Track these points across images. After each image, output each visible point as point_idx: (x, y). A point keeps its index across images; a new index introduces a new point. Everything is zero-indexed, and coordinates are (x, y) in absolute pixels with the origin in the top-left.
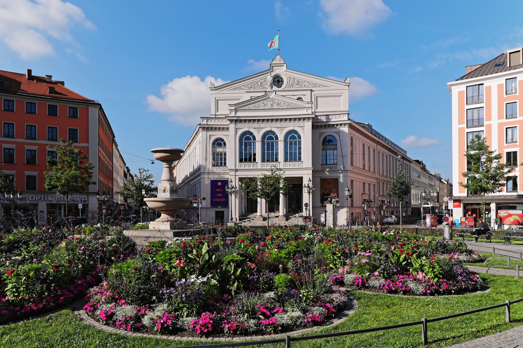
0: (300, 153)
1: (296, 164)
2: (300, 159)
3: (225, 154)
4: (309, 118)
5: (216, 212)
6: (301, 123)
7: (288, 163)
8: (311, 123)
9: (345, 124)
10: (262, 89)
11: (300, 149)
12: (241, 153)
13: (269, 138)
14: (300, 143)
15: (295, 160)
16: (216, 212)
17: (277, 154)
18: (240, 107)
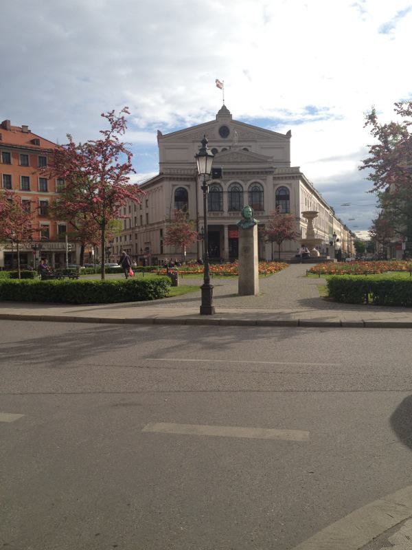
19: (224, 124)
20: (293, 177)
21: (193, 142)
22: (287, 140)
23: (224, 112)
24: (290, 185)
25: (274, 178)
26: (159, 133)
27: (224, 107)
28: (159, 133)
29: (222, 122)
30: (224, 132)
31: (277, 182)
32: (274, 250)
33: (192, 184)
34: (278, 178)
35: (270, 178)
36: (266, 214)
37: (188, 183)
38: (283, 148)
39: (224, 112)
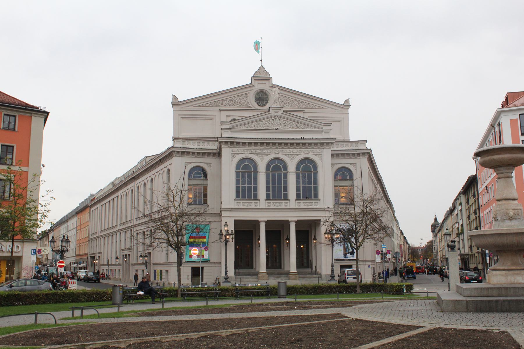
0: (316, 189)
1: (313, 204)
2: (316, 196)
3: (205, 189)
4: (328, 144)
5: (192, 268)
6: (317, 150)
7: (302, 201)
8: (330, 150)
9: (363, 154)
10: (240, 107)
11: (316, 183)
12: (238, 188)
13: (277, 168)
14: (316, 174)
15: (310, 198)
16: (192, 268)
17: (286, 189)
18: (238, 126)
19: (261, 92)
20: (359, 154)
21: (220, 110)
22: (344, 111)
23: (262, 76)
24: (354, 164)
25: (333, 155)
26: (175, 97)
27: (262, 67)
28: (175, 97)
29: (259, 86)
30: (262, 98)
31: (336, 161)
32: (335, 258)
33: (214, 161)
34: (338, 155)
35: (327, 153)
36: (321, 205)
37: (208, 160)
38: (339, 121)
39: (262, 76)
